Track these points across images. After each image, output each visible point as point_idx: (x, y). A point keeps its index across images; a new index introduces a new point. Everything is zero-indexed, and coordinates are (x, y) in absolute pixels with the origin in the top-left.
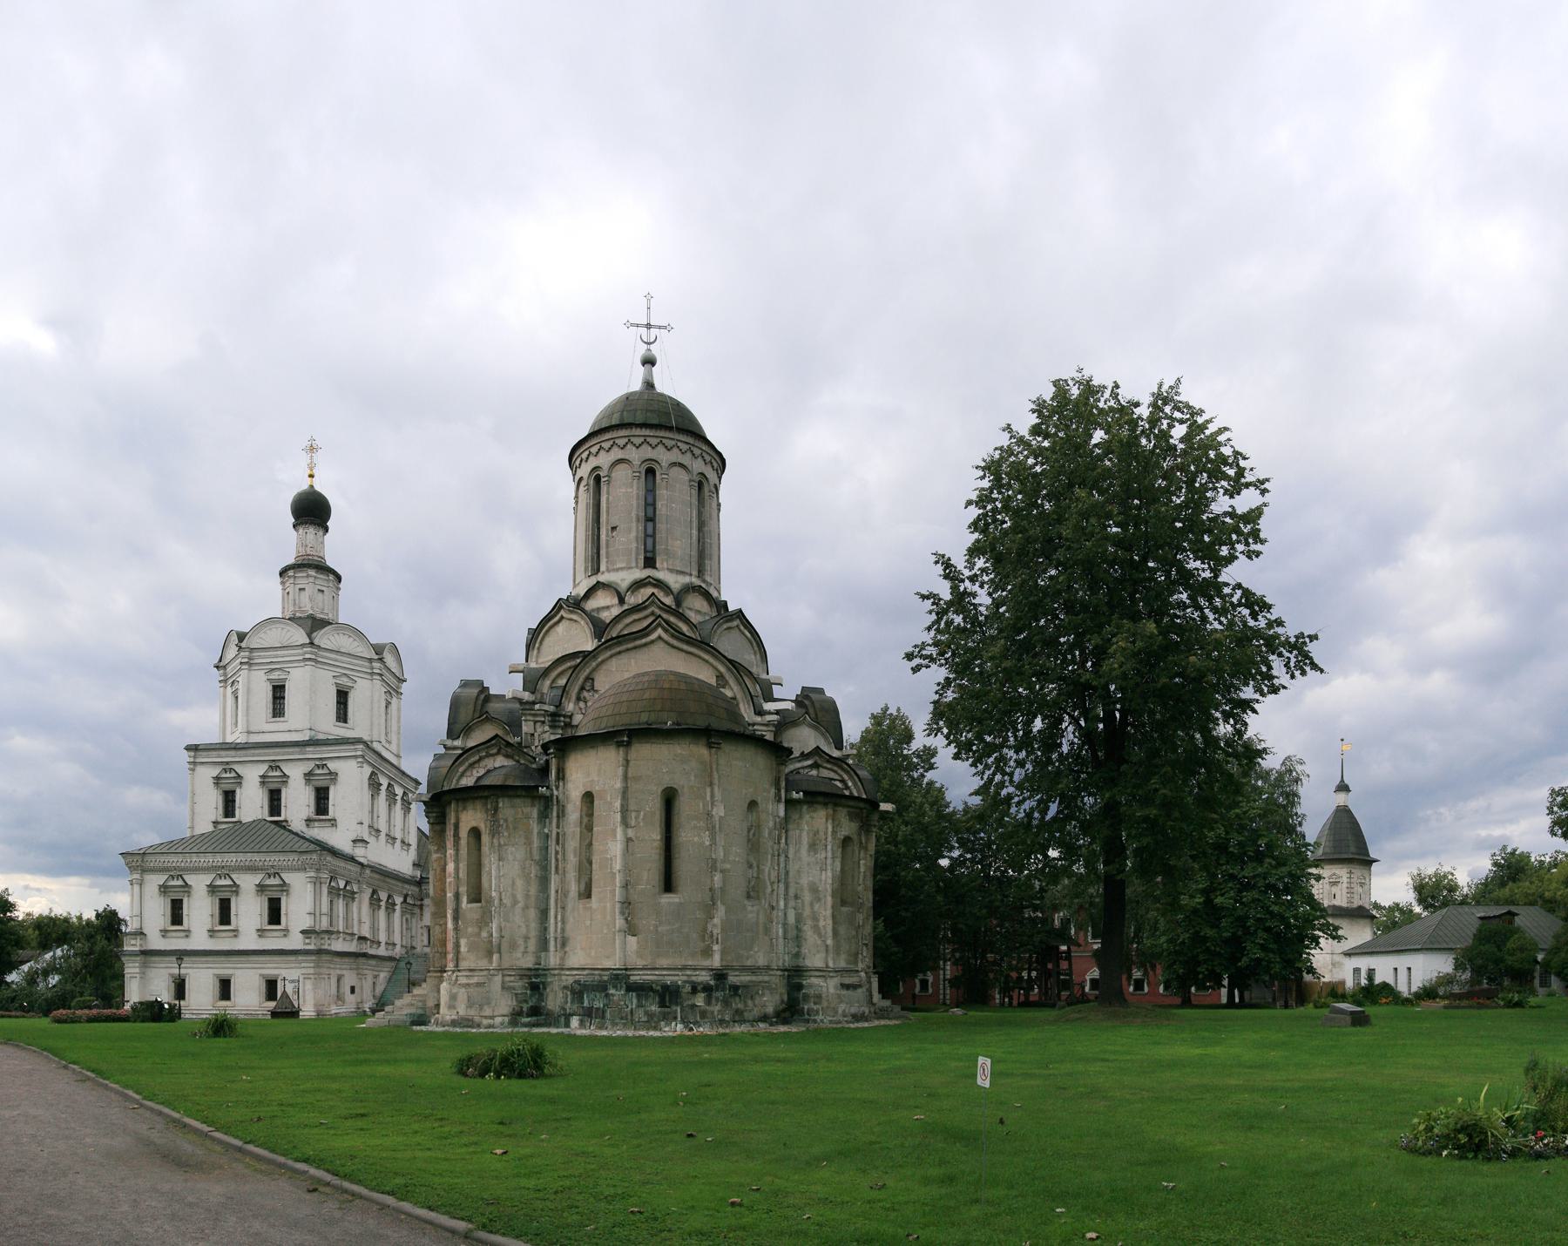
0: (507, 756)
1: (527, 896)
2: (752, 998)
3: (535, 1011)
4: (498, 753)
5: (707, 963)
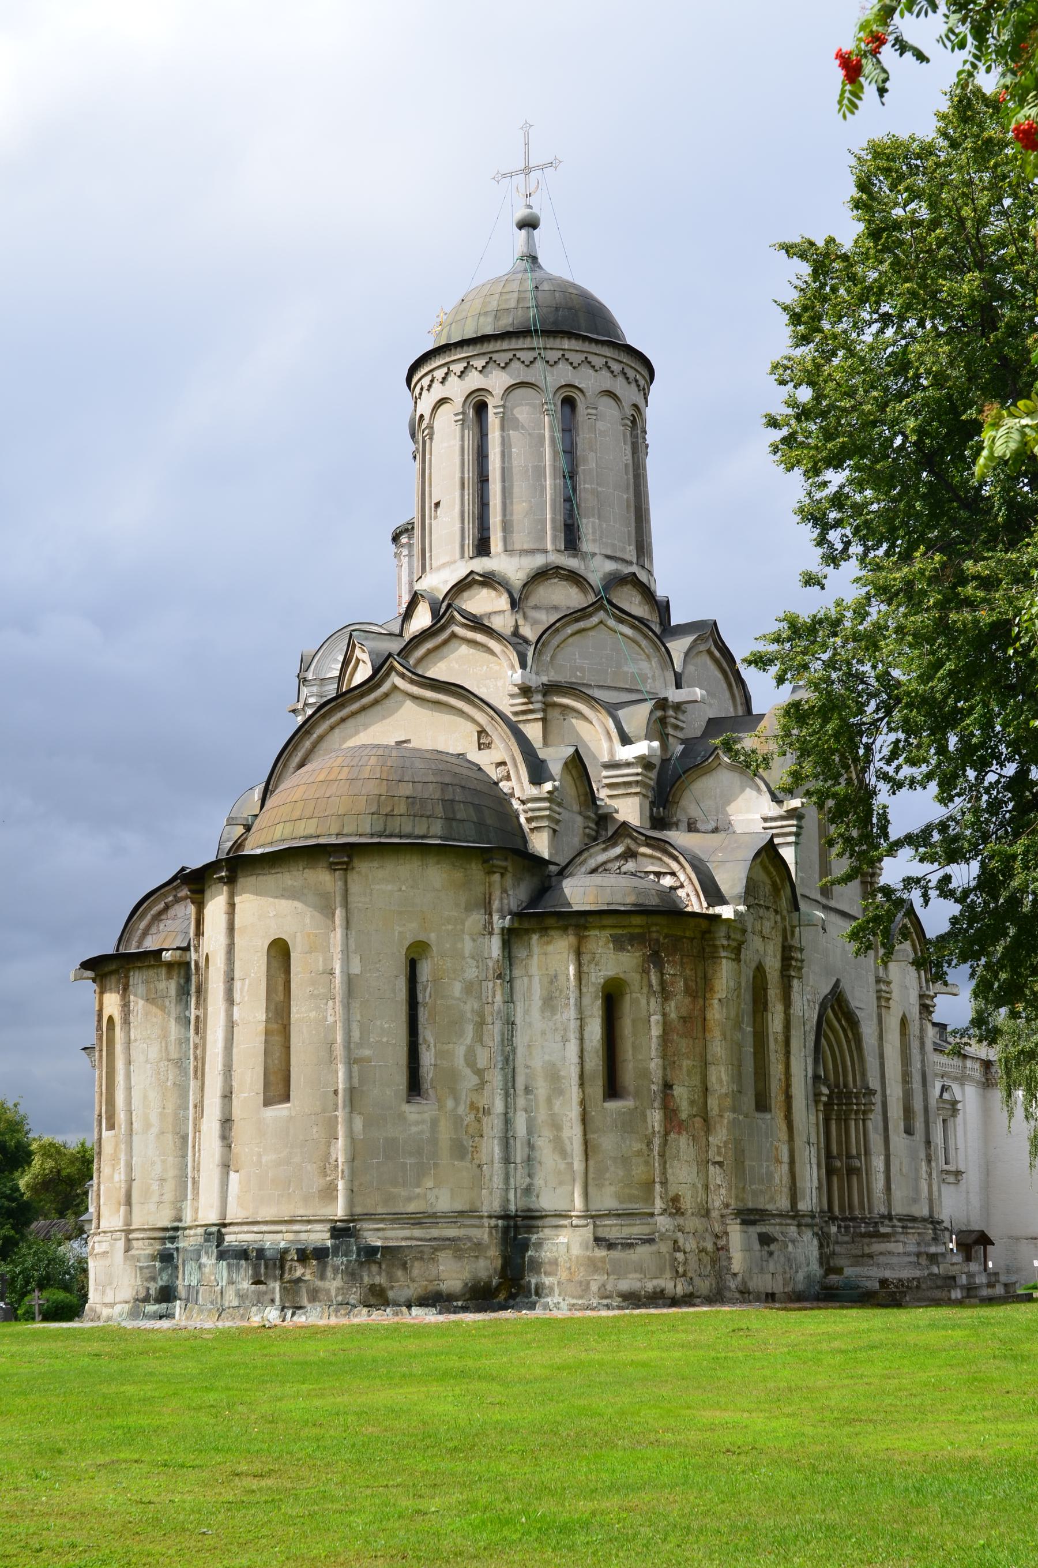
1: (162, 1116)
2: (404, 1266)
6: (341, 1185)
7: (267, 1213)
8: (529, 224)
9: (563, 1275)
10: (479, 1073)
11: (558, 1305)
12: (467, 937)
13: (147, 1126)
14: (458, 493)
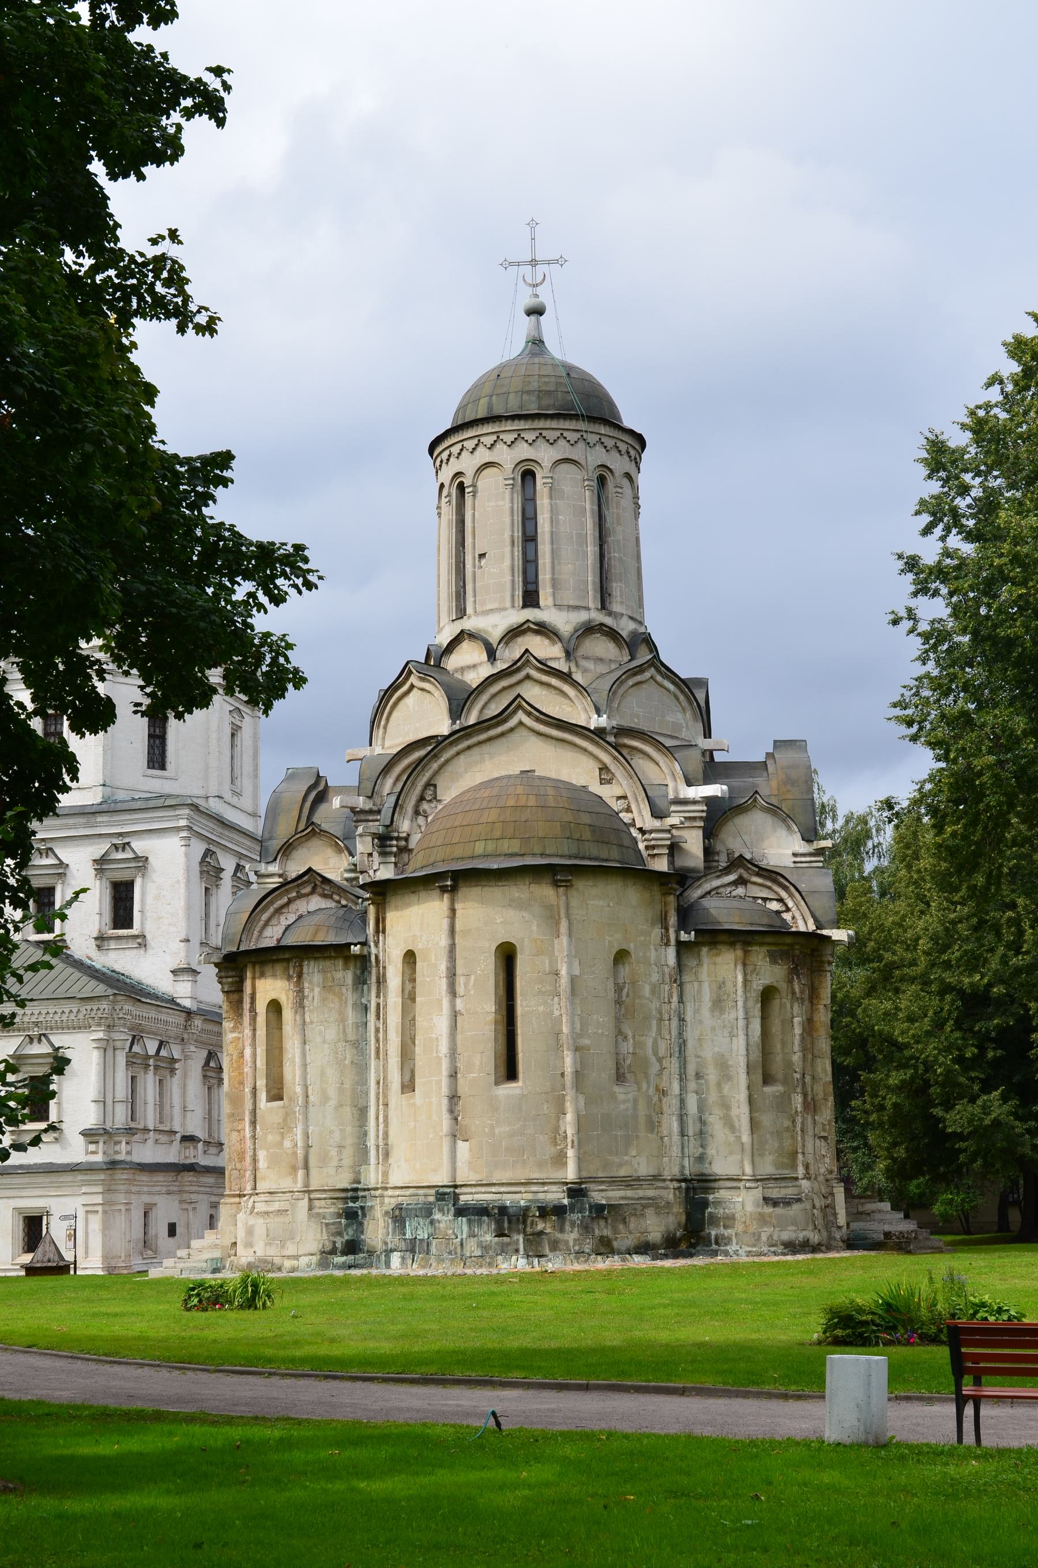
0: (324, 896)
1: (341, 1090)
2: (624, 1221)
3: (352, 1247)
4: (312, 892)
5: (557, 1175)
6: (571, 1153)
7: (499, 1176)
8: (536, 311)
9: (739, 1227)
10: (660, 1060)
11: (739, 1252)
12: (652, 947)
13: (325, 1098)
14: (508, 549)
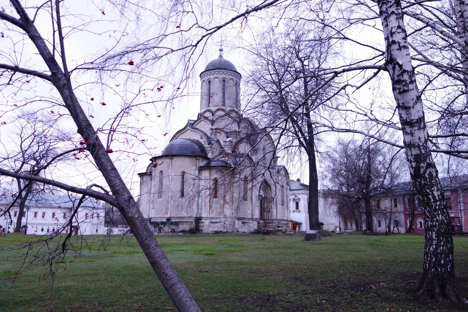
8: (221, 50)
